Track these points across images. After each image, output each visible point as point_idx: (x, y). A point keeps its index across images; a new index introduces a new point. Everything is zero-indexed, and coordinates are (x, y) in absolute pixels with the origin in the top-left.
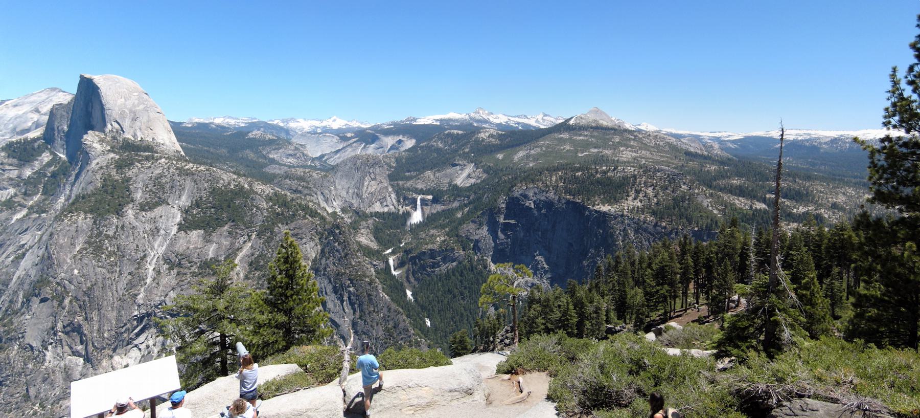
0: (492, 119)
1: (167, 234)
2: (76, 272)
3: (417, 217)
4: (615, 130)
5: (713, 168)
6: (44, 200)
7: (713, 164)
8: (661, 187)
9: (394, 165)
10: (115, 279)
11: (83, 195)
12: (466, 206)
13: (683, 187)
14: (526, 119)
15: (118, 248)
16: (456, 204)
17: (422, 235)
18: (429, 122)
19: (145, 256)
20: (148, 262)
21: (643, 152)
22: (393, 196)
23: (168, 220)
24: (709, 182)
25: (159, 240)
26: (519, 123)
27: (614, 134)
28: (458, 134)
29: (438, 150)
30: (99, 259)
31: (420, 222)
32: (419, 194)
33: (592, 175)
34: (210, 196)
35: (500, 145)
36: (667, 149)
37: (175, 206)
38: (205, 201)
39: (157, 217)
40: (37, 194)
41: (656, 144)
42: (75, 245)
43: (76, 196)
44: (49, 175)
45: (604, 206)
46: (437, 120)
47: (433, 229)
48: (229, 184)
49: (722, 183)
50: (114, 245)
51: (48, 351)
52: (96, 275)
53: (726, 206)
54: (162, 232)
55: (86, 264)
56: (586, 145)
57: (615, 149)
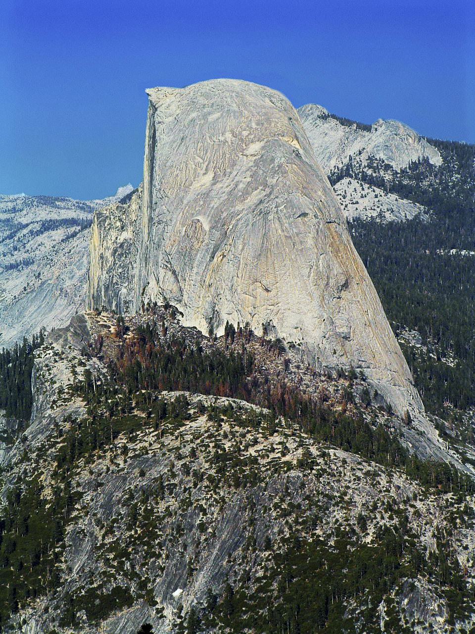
34: (275, 574)
38: (252, 597)
48: (363, 521)
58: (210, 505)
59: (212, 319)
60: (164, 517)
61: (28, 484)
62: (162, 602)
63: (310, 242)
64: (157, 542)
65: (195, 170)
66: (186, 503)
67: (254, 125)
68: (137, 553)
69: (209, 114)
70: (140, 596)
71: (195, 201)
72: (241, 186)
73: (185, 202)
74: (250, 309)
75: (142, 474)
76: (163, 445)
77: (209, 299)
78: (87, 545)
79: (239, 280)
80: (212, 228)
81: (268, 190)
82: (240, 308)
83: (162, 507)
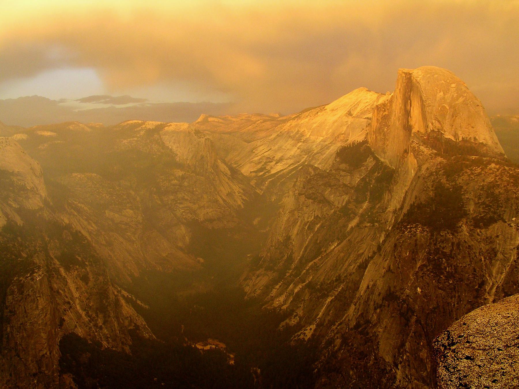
1: (506, 260)
2: (419, 290)
6: (371, 208)
10: (454, 305)
11: (418, 204)
15: (455, 269)
19: (483, 284)
20: (487, 290)
23: (505, 241)
25: (497, 265)
30: (439, 280)
37: (512, 225)
39: (493, 237)
40: (363, 202)
42: (415, 261)
43: (411, 206)
44: (374, 181)
50: (451, 266)
51: (398, 369)
52: (436, 297)
54: (500, 256)
55: (428, 284)
58: (517, 191)
59: (456, 135)
60: (499, 195)
61: (437, 182)
62: (508, 221)
63: (482, 114)
64: (500, 202)
65: (436, 91)
66: (507, 191)
67: (450, 79)
68: (494, 205)
69: (434, 75)
70: (500, 220)
71: (440, 100)
72: (455, 96)
73: (437, 100)
74: (468, 133)
75: (484, 181)
76: (486, 172)
77: (453, 130)
78: (472, 202)
79: (463, 124)
80: (449, 108)
81: (465, 98)
82: (464, 133)
83: (497, 191)
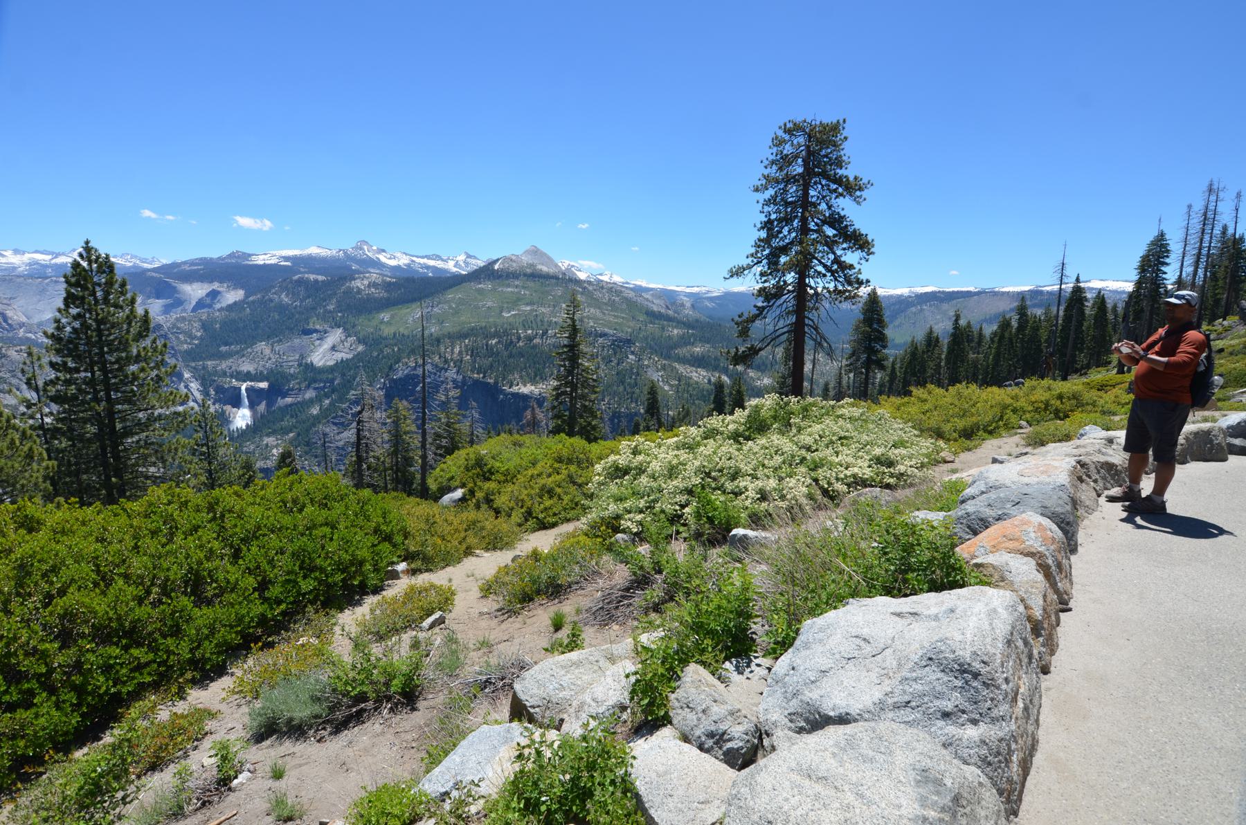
0: (383, 258)
3: (242, 418)
4: (557, 278)
5: (676, 331)
7: (676, 327)
8: (603, 359)
9: (199, 334)
12: (327, 396)
13: (630, 357)
14: (439, 262)
16: (310, 394)
17: (249, 447)
18: (273, 261)
21: (592, 310)
22: (194, 386)
24: (666, 350)
26: (428, 267)
27: (557, 285)
28: (316, 281)
29: (282, 308)
31: (247, 425)
32: (245, 381)
33: (512, 342)
35: (388, 299)
36: (624, 306)
41: (610, 299)
45: (525, 386)
46: (286, 258)
47: (268, 435)
49: (683, 351)
53: (679, 381)
56: (516, 301)
57: (554, 306)
